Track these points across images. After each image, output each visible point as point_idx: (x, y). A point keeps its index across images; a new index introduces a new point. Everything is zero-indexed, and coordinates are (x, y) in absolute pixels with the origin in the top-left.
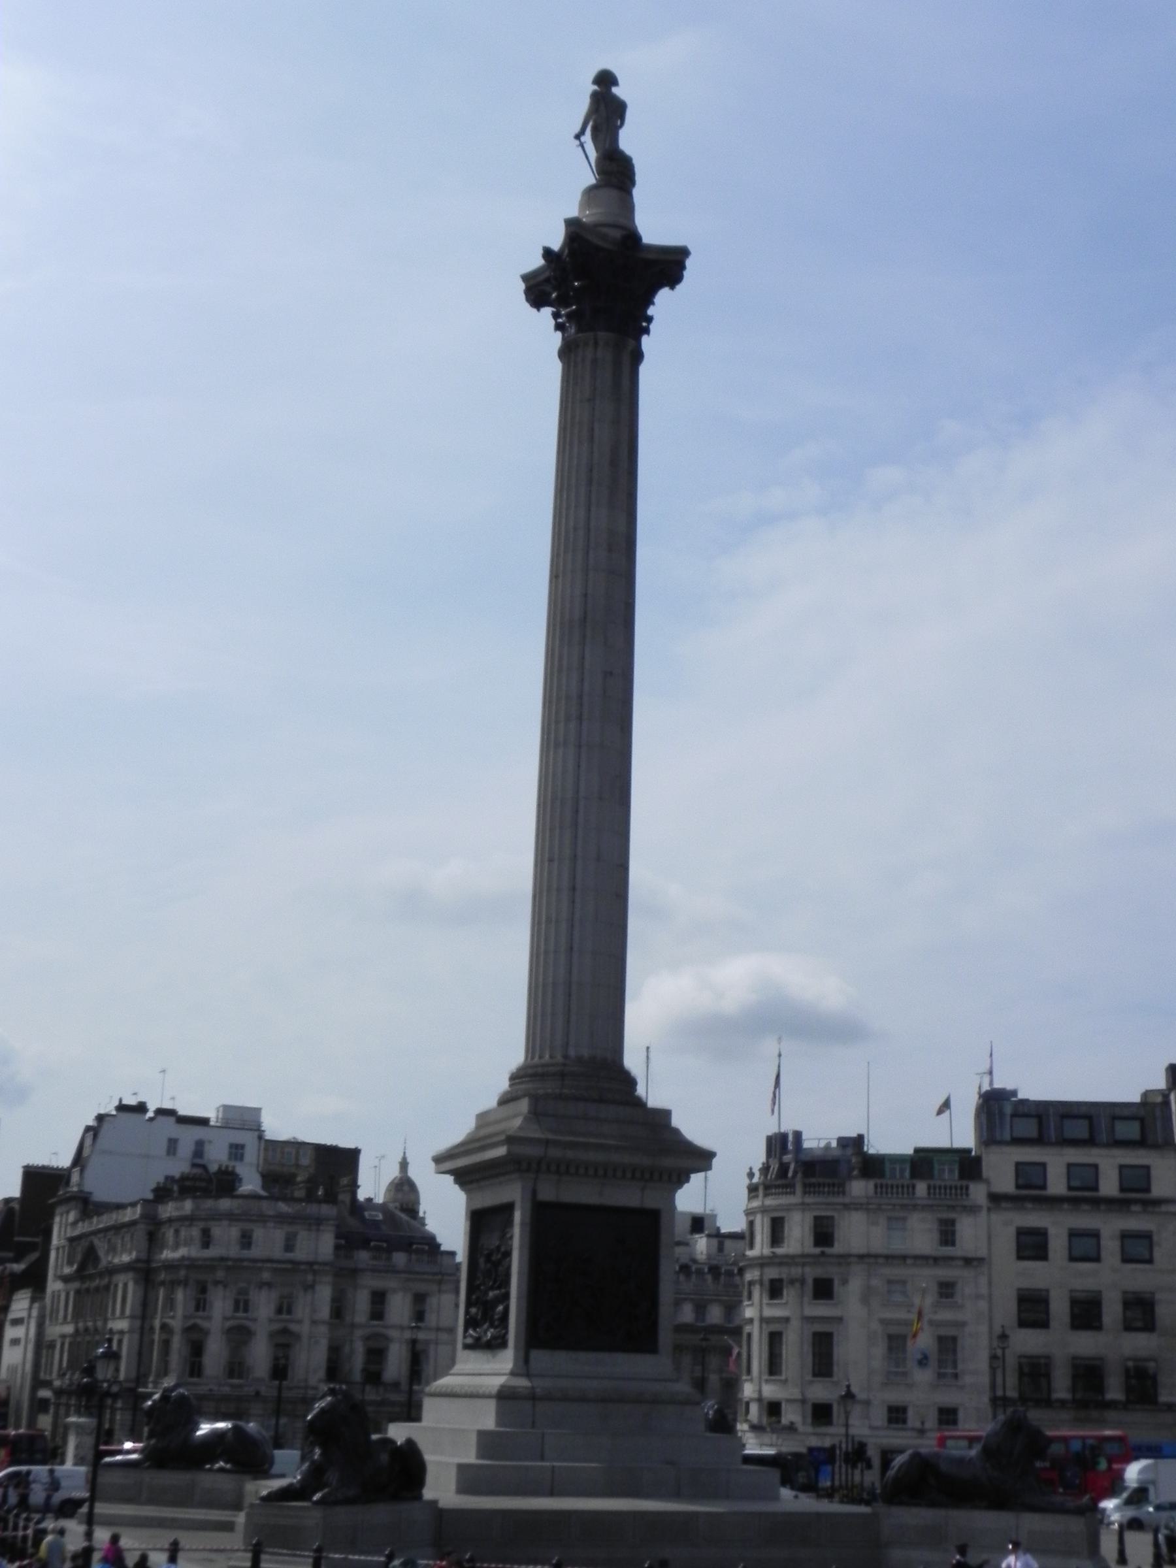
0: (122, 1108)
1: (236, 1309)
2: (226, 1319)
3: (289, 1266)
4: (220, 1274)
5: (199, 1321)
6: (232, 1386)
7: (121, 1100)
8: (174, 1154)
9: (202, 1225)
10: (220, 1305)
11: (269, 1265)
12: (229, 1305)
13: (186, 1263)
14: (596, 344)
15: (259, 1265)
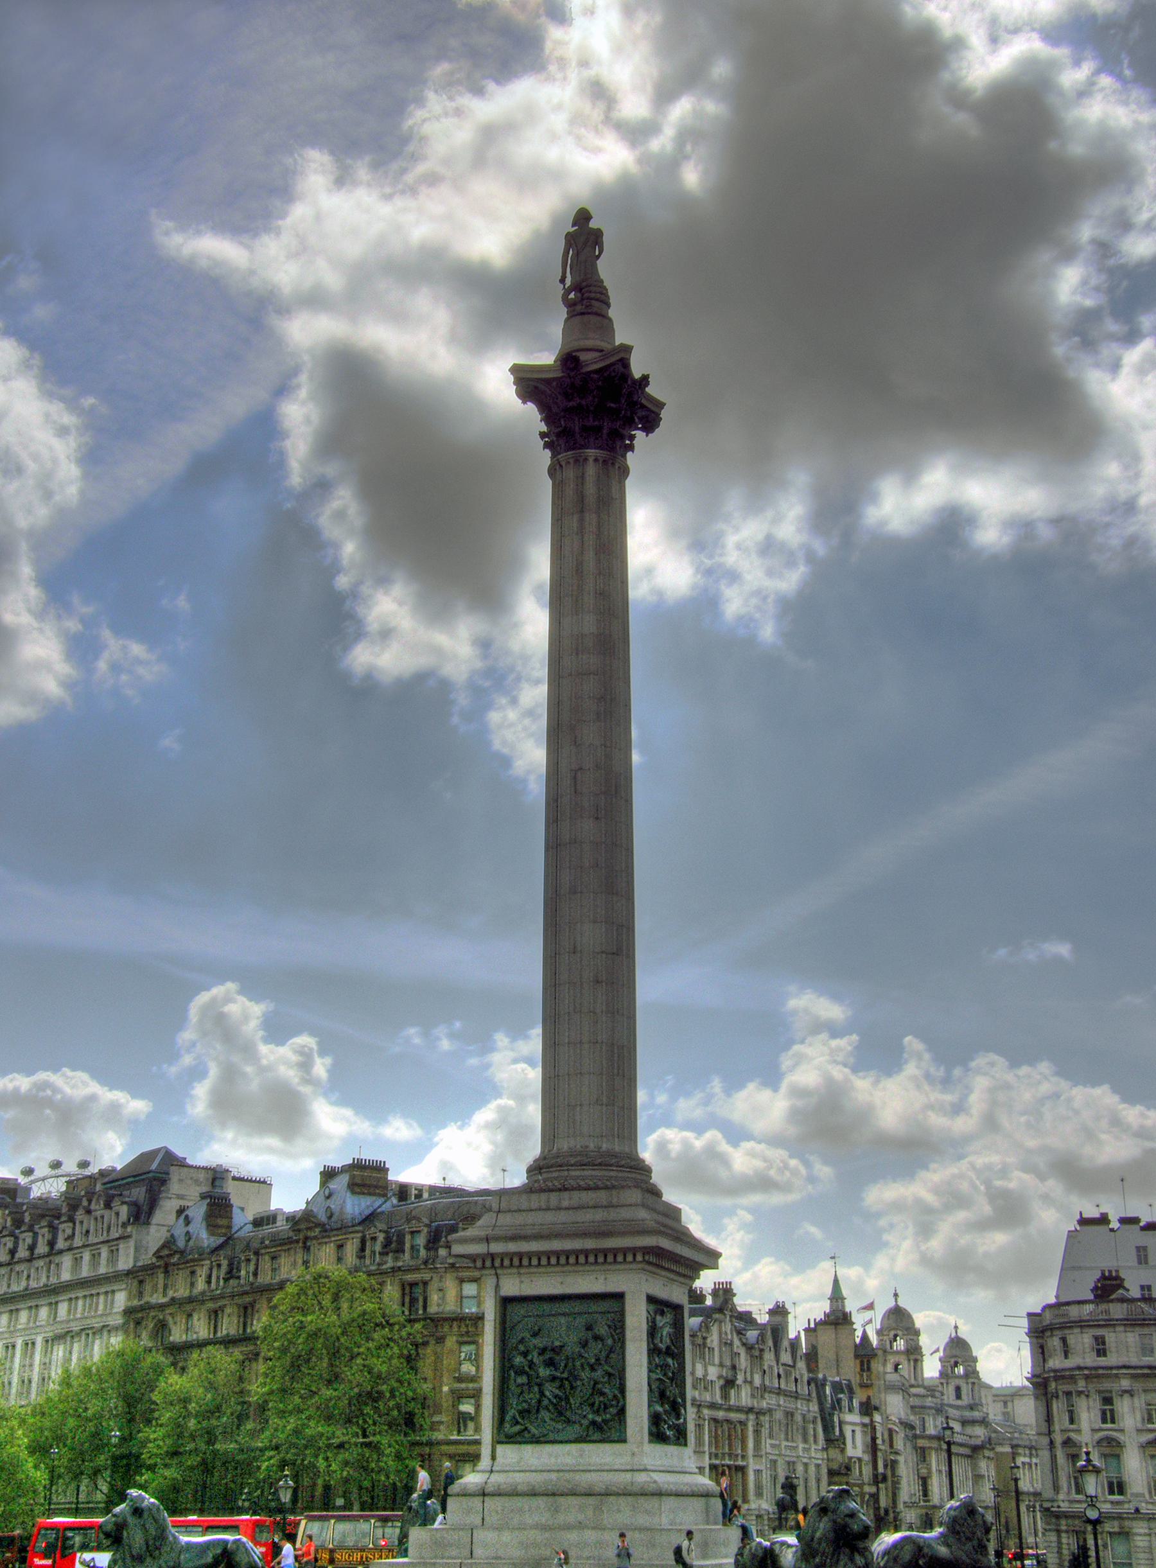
0: (1084, 1221)
1: (1104, 1421)
2: (1094, 1430)
3: (1146, 1371)
4: (1081, 1385)
5: (1073, 1435)
6: (1112, 1503)
7: (1081, 1213)
8: (1146, 1263)
9: (1058, 1333)
10: (1088, 1415)
11: (1124, 1371)
12: (1096, 1415)
13: (1052, 1374)
14: (561, 466)
15: (1114, 1372)
